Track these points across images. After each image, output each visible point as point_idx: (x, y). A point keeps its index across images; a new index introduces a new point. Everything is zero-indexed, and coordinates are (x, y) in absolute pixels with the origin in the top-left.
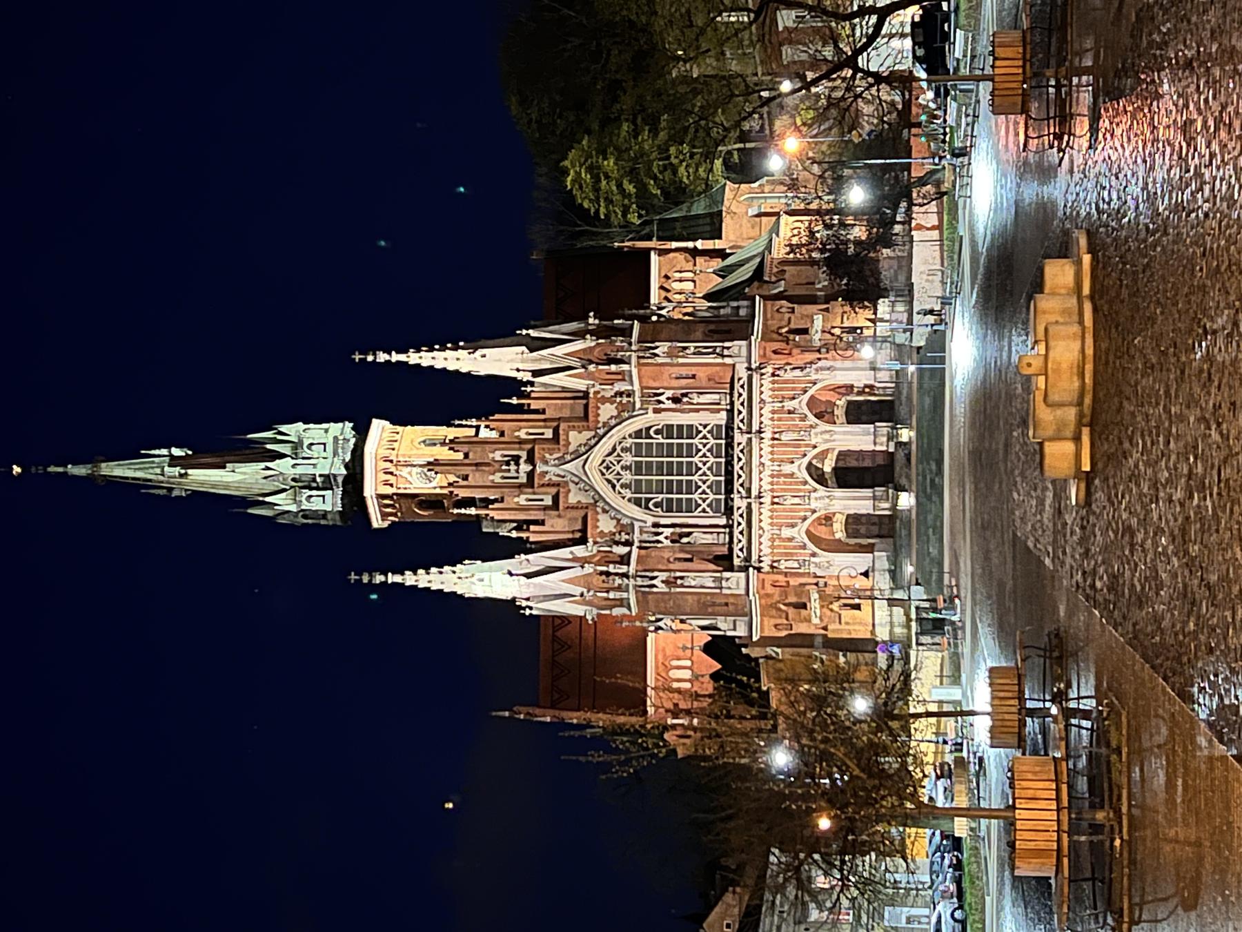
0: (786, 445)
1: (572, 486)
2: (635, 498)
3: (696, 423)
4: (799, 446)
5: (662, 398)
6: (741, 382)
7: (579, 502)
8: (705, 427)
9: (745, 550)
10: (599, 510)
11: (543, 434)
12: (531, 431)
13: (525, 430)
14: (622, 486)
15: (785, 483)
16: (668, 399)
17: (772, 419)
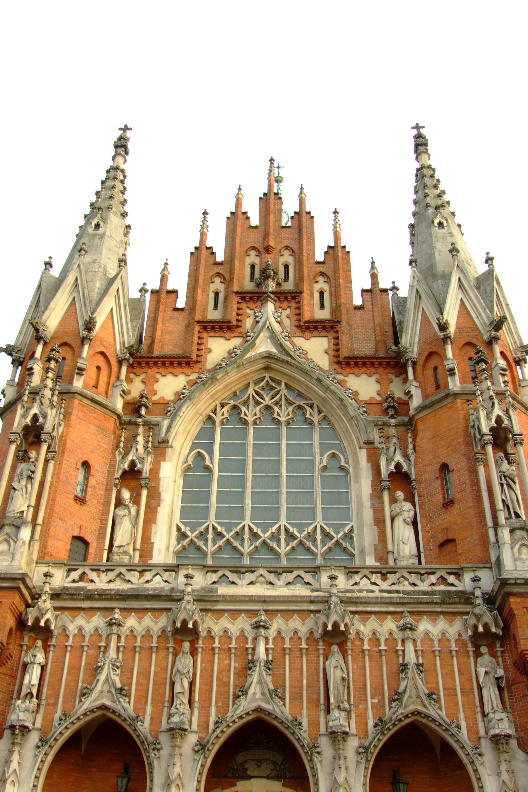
0: (313, 674)
1: (236, 342)
2: (213, 429)
3: (354, 523)
4: (314, 702)
5: (399, 458)
6: (451, 579)
7: (210, 351)
8: (349, 536)
9: (81, 584)
10: (193, 377)
11: (322, 306)
12: (326, 296)
13: (326, 287)
14: (235, 407)
15: (225, 670)
16: (398, 466)
17: (375, 639)
